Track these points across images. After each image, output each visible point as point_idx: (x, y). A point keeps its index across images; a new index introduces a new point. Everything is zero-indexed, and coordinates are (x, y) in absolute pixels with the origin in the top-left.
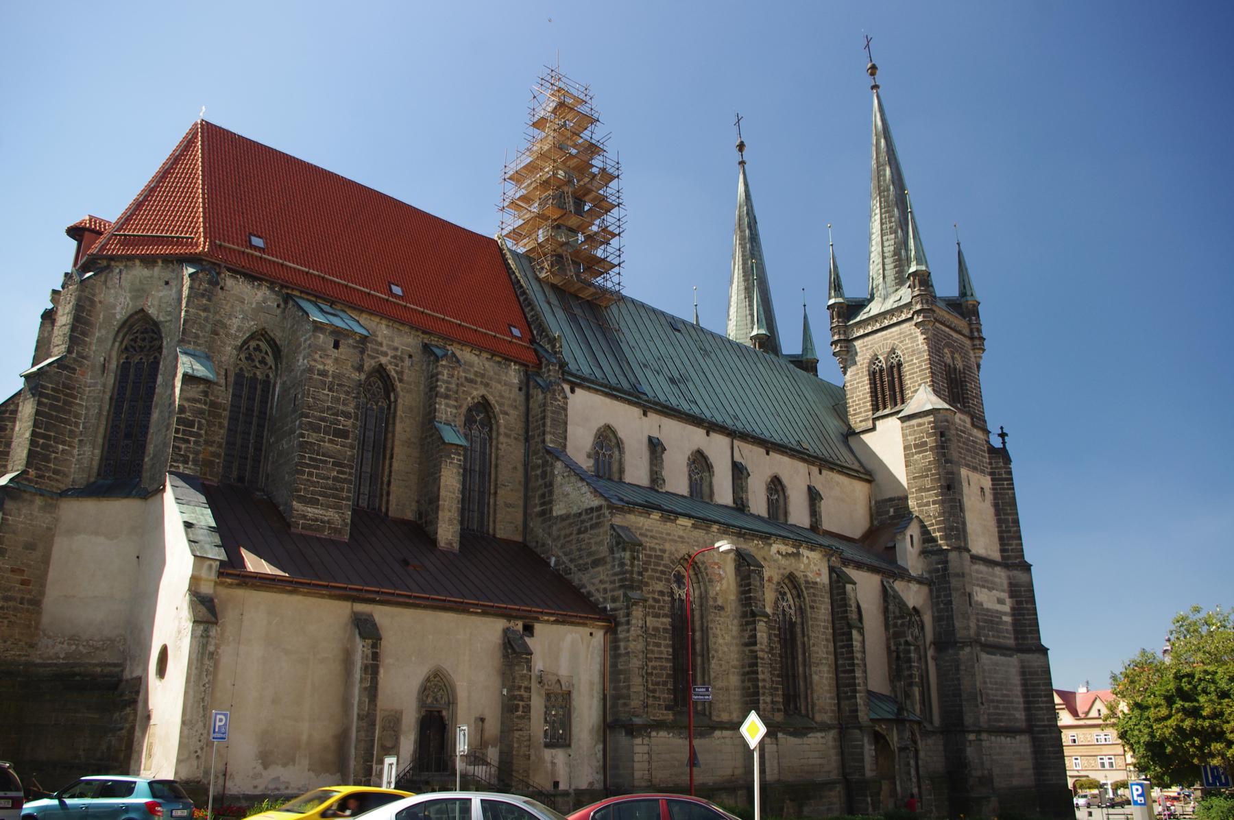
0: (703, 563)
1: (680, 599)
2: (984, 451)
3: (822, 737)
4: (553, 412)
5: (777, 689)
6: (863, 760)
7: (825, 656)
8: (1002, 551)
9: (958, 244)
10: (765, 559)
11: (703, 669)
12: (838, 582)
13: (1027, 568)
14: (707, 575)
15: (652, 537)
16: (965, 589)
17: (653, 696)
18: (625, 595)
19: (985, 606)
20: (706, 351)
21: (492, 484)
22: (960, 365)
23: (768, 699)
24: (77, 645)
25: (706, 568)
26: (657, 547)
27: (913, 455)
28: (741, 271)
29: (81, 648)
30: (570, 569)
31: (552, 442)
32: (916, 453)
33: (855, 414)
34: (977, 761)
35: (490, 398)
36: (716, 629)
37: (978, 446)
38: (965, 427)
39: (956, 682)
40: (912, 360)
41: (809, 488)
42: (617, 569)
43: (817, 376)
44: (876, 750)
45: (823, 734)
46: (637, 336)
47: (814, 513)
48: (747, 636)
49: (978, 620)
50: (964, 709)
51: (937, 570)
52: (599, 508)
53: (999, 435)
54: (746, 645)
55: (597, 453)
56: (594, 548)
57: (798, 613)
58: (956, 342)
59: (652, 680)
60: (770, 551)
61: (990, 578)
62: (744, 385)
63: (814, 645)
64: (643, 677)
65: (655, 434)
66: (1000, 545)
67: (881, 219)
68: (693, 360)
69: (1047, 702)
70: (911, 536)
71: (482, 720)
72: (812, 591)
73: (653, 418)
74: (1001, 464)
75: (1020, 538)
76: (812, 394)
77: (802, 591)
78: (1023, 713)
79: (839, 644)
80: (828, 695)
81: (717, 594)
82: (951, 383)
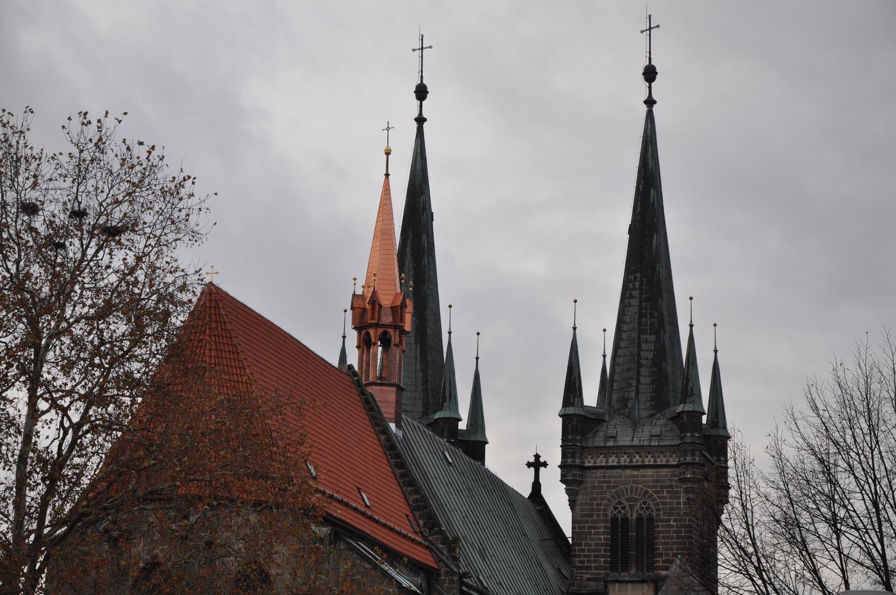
40: (669, 520)
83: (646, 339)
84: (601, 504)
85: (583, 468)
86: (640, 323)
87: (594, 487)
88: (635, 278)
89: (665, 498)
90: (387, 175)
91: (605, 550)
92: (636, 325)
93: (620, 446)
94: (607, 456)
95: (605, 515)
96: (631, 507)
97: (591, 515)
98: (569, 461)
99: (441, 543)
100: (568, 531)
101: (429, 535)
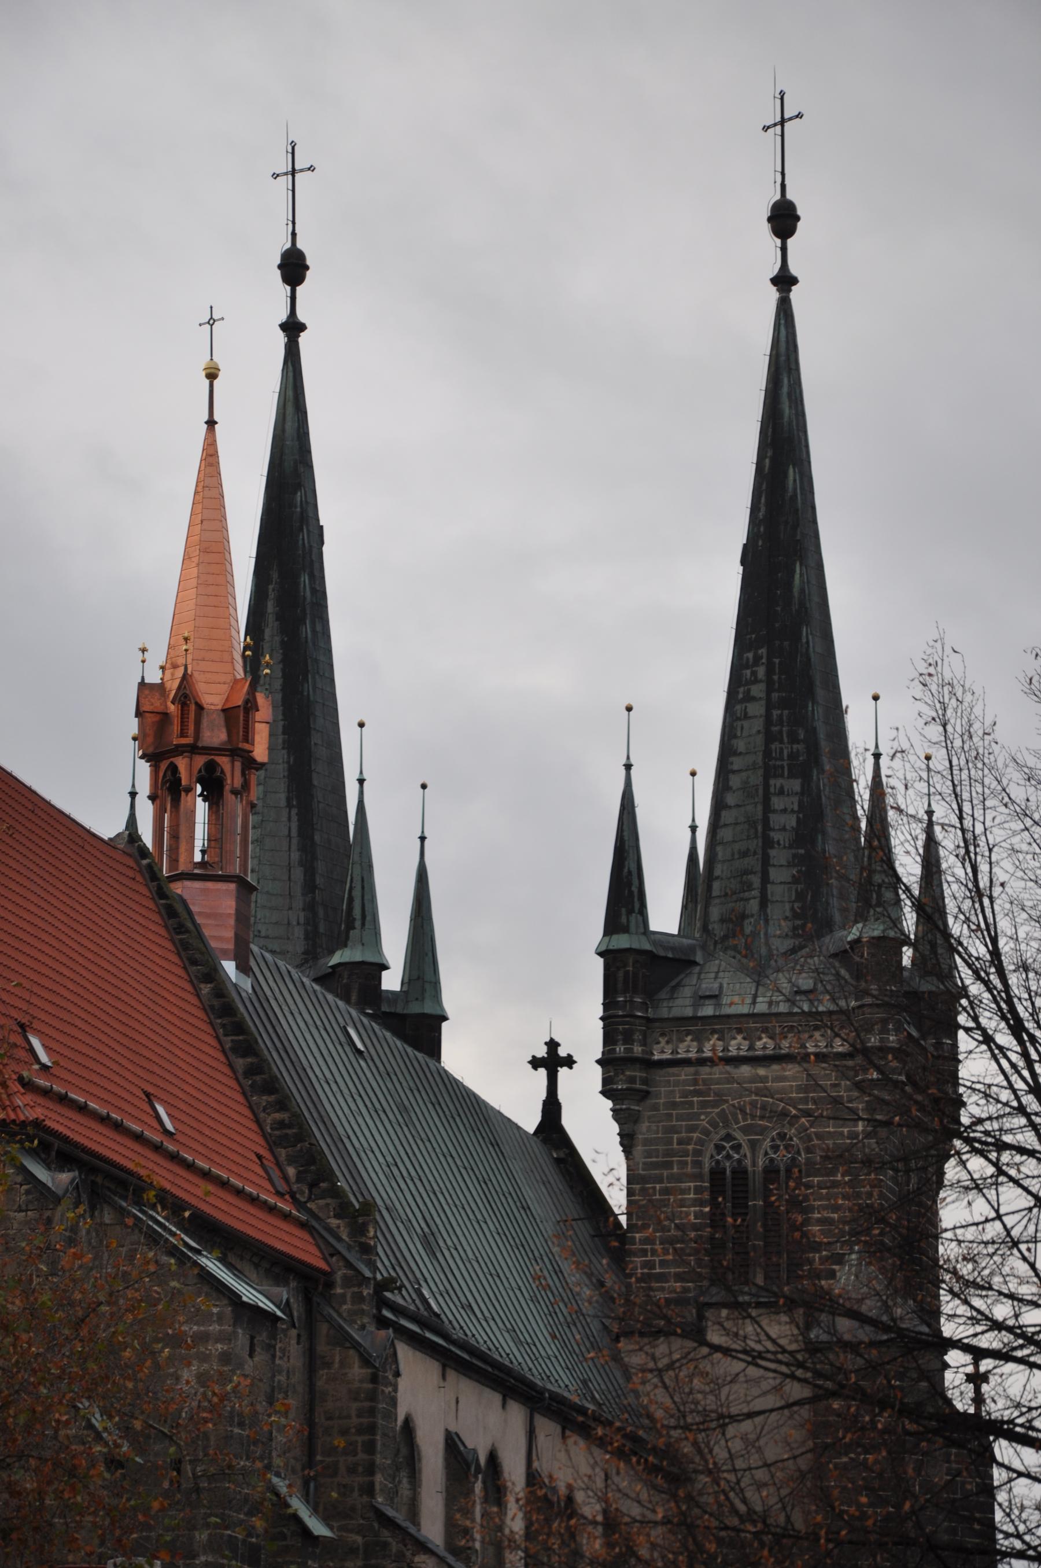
65: (453, 1428)
83: (782, 787)
84: (688, 1141)
85: (649, 1064)
86: (767, 754)
87: (674, 1105)
88: (757, 659)
90: (211, 423)
92: (759, 759)
93: (729, 1016)
94: (700, 1038)
95: (698, 1164)
96: (753, 1145)
97: (668, 1165)
98: (620, 1049)
99: (336, 1216)
100: (617, 1198)
101: (309, 1199)
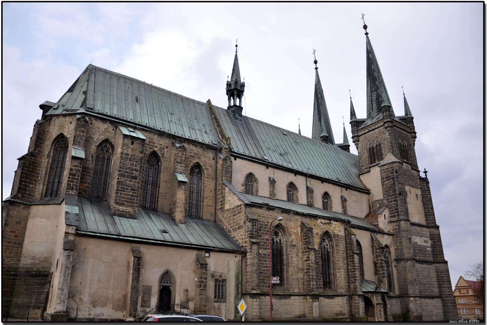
0: (286, 227)
1: (277, 242)
2: (417, 179)
3: (341, 299)
4: (226, 168)
5: (320, 279)
6: (359, 309)
7: (343, 265)
8: (426, 220)
9: (404, 94)
10: (315, 225)
11: (287, 271)
12: (348, 234)
13: (438, 227)
14: (288, 232)
15: (263, 217)
16: (408, 237)
17: (263, 282)
18: (250, 240)
19: (418, 244)
20: (297, 142)
21: (202, 197)
22: (406, 144)
23: (315, 283)
24: (35, 260)
25: (288, 229)
26: (265, 221)
27: (385, 181)
28: (317, 111)
29: (36, 261)
30: (231, 231)
31: (225, 180)
32: (386, 180)
33: (362, 166)
34: (414, 309)
35: (200, 163)
36: (292, 254)
37: (414, 177)
38: (408, 169)
39: (405, 276)
40: (384, 143)
41: (341, 197)
42: (247, 230)
43: (349, 152)
44: (365, 304)
45: (342, 298)
46: (267, 137)
47: (344, 207)
48: (306, 257)
49: (414, 250)
50: (408, 287)
51: (396, 229)
52: (241, 205)
53: (424, 172)
54: (306, 261)
55: (246, 184)
56: (239, 222)
57: (331, 247)
58: (403, 134)
59: (263, 276)
60: (317, 222)
61: (421, 232)
62: (314, 156)
63: (337, 261)
64: (257, 274)
65: (272, 176)
66: (426, 218)
67: (371, 86)
68: (291, 146)
69: (448, 284)
70: (385, 215)
71: (187, 291)
72: (336, 238)
73: (271, 170)
74: (425, 184)
75: (434, 215)
76: (345, 159)
77: (332, 239)
78: (437, 289)
79: (349, 260)
80: (344, 282)
81: (293, 240)
82: (402, 151)
85: (358, 136)
87: (362, 141)
89: (382, 136)
90: (236, 52)
91: (368, 158)
95: (367, 148)
